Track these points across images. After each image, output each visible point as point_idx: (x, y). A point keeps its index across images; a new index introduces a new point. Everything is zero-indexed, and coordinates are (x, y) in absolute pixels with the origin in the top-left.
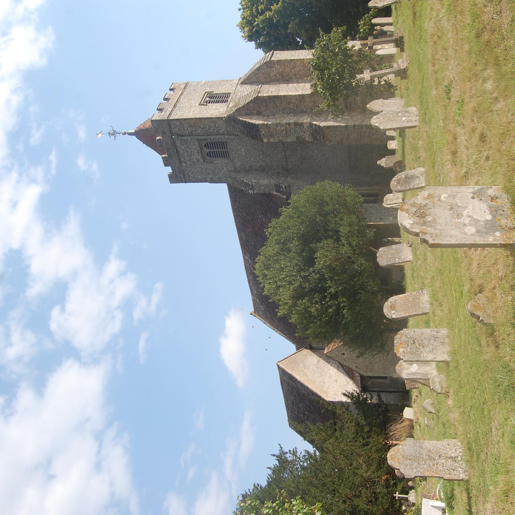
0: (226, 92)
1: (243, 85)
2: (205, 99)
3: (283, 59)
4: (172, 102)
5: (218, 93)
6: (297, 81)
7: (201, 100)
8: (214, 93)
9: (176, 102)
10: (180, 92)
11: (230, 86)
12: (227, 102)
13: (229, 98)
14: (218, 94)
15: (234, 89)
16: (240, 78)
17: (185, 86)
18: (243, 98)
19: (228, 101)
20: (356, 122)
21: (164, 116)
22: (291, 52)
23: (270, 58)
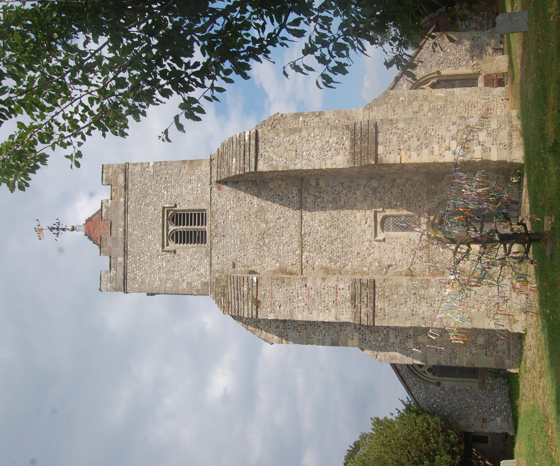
0: (197, 207)
1: (222, 186)
2: (168, 230)
3: (280, 169)
4: (117, 233)
5: (184, 208)
6: (317, 184)
7: (161, 231)
8: (178, 208)
9: (125, 239)
10: (122, 200)
11: (199, 185)
12: (205, 243)
13: (205, 225)
14: (185, 210)
15: (208, 196)
16: (211, 160)
17: (125, 181)
18: (232, 286)
19: (205, 232)
20: (442, 356)
21: (118, 283)
22: (293, 137)
23: (256, 167)
